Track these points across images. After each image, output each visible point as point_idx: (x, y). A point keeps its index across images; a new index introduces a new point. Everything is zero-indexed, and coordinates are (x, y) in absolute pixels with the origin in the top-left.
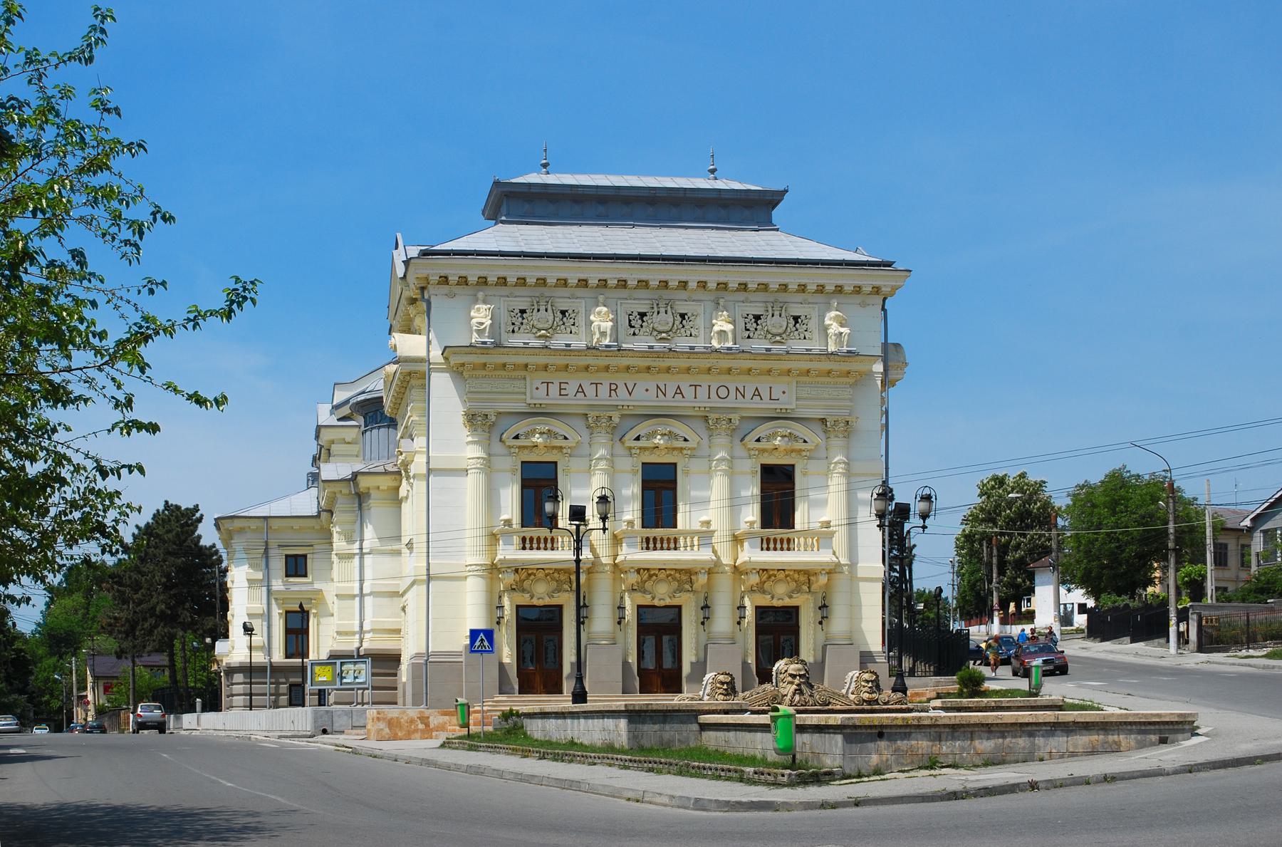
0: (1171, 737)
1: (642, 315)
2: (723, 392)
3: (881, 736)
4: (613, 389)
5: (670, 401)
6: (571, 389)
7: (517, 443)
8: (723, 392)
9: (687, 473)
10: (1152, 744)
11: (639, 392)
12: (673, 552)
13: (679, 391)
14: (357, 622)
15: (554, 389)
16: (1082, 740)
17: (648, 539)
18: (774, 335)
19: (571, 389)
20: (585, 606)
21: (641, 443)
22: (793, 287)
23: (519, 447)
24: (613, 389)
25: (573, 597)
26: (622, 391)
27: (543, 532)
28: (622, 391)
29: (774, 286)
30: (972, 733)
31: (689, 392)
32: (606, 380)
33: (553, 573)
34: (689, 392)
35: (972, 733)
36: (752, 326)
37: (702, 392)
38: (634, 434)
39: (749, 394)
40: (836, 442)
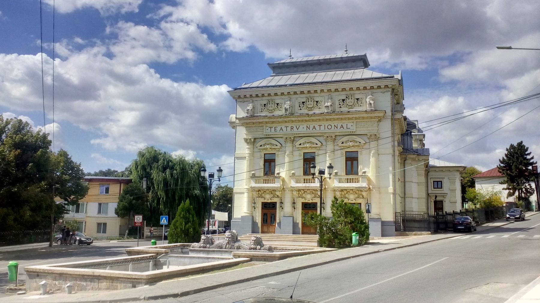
1: (303, 103)
2: (330, 127)
3: (38, 276)
4: (292, 128)
5: (311, 131)
6: (278, 129)
7: (261, 148)
8: (330, 127)
9: (361, 154)
10: (129, 288)
12: (357, 184)
13: (314, 127)
15: (273, 129)
16: (104, 284)
17: (348, 179)
20: (324, 203)
21: (301, 146)
23: (302, 148)
24: (292, 128)
25: (319, 199)
26: (295, 129)
27: (310, 177)
28: (295, 129)
29: (348, 89)
31: (317, 128)
32: (290, 125)
33: (313, 191)
34: (317, 128)
39: (339, 127)
40: (373, 144)
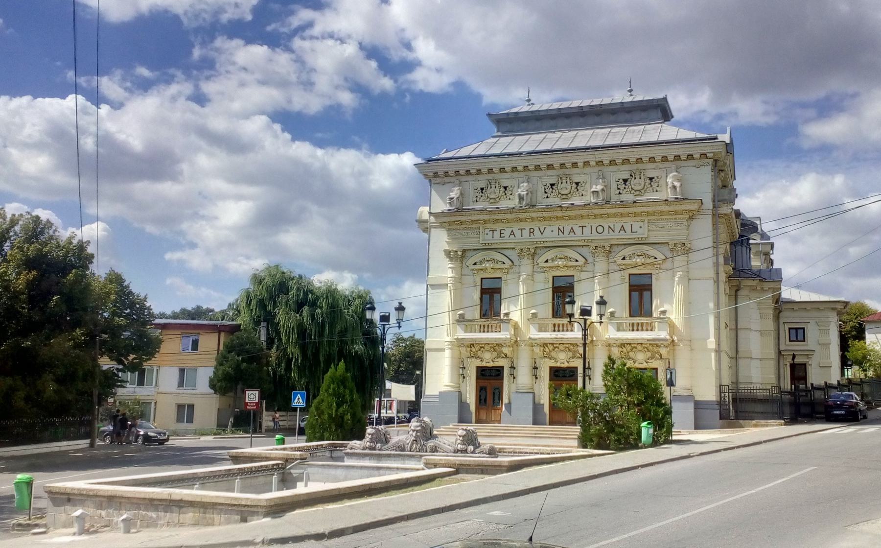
0: (249, 518)
1: (552, 185)
2: (600, 229)
3: (69, 500)
4: (532, 232)
5: (566, 236)
6: (507, 233)
7: (476, 267)
8: (600, 229)
9: (657, 279)
10: (236, 522)
11: (547, 233)
12: (649, 333)
13: (572, 230)
14: (164, 391)
15: (497, 234)
16: (189, 516)
17: (633, 324)
18: (636, 191)
19: (507, 233)
20: (589, 368)
21: (549, 264)
22: (645, 159)
23: (550, 267)
24: (532, 232)
25: (581, 361)
26: (537, 232)
27: (566, 321)
28: (537, 232)
29: (633, 160)
30: (120, 503)
31: (578, 231)
32: (527, 226)
33: (570, 346)
34: (578, 231)
35: (120, 503)
36: (622, 187)
37: (587, 231)
38: (544, 258)
39: (617, 229)
40: (679, 260)
